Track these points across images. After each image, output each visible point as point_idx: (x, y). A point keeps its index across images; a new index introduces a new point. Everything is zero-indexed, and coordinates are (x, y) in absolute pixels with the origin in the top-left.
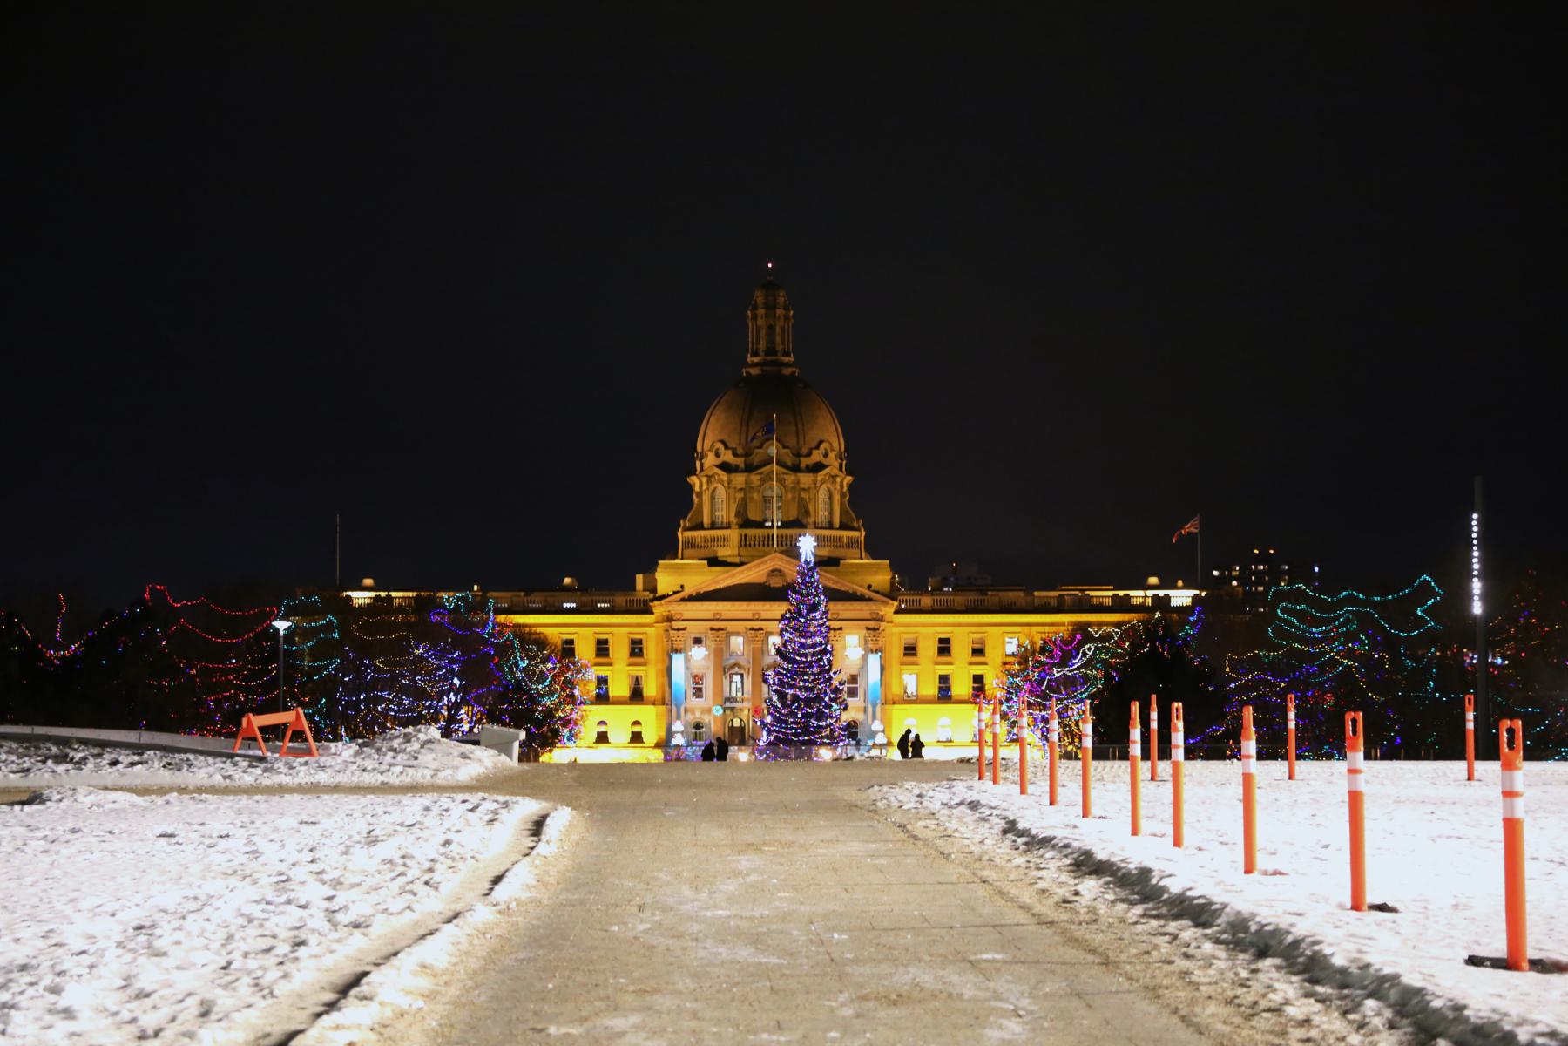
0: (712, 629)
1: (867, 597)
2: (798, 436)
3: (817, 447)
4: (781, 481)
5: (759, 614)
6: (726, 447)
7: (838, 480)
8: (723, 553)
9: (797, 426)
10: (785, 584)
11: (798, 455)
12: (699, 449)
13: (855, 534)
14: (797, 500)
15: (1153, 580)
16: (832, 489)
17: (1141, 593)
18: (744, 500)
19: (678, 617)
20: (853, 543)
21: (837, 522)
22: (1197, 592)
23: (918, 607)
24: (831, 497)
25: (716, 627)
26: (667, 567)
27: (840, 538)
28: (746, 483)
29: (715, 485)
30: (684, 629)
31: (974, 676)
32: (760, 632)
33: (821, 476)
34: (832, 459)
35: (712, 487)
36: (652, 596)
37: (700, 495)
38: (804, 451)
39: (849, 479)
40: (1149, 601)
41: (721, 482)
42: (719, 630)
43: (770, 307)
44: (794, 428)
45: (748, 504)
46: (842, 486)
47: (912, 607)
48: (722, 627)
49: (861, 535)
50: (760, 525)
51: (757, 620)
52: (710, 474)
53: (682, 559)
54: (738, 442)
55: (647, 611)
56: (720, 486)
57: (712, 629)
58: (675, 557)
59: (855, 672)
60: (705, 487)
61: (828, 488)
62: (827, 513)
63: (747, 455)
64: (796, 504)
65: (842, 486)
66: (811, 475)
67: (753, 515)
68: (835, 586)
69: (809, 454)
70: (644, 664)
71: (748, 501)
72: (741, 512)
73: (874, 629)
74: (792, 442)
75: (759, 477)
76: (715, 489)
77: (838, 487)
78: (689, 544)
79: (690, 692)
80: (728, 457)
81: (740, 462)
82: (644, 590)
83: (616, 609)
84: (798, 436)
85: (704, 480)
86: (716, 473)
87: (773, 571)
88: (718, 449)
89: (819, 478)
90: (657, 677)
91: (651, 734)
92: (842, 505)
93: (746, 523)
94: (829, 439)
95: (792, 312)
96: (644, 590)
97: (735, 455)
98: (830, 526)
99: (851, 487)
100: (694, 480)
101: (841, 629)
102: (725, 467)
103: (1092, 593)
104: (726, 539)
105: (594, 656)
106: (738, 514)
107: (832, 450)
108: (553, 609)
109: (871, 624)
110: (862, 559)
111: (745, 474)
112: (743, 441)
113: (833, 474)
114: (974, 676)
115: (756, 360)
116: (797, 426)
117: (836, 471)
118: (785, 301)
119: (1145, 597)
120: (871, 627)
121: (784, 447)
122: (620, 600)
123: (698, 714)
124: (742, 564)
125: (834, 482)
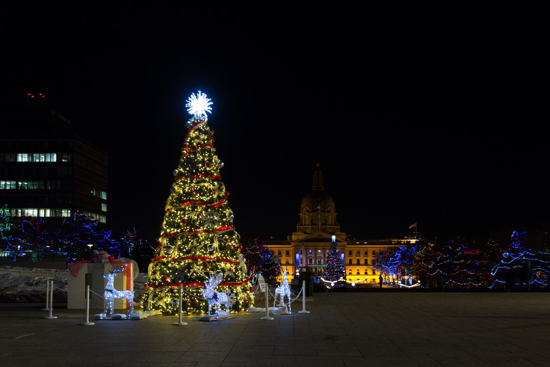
3: (329, 207)
6: (308, 207)
7: (334, 214)
8: (308, 231)
12: (302, 207)
13: (338, 227)
15: (406, 237)
17: (403, 240)
20: (337, 229)
21: (333, 224)
22: (416, 240)
24: (332, 218)
26: (294, 234)
27: (334, 227)
30: (299, 248)
33: (330, 213)
34: (332, 209)
36: (291, 241)
37: (302, 218)
38: (326, 208)
39: (336, 214)
40: (405, 242)
41: (307, 215)
46: (334, 216)
49: (339, 227)
50: (316, 225)
51: (316, 246)
53: (298, 232)
55: (290, 244)
58: (296, 232)
60: (303, 216)
61: (332, 216)
62: (331, 222)
65: (334, 216)
67: (314, 222)
69: (327, 208)
70: (290, 256)
72: (311, 222)
73: (343, 249)
76: (305, 216)
77: (334, 216)
78: (299, 229)
81: (311, 210)
82: (289, 239)
85: (303, 214)
90: (292, 259)
91: (291, 273)
92: (334, 220)
93: (313, 224)
94: (332, 206)
96: (289, 239)
97: (310, 208)
98: (332, 225)
99: (337, 216)
100: (301, 214)
102: (308, 211)
103: (393, 240)
104: (308, 228)
106: (311, 222)
109: (342, 247)
110: (339, 232)
115: (315, 187)
117: (333, 212)
119: (404, 241)
121: (322, 207)
122: (284, 242)
124: (312, 234)
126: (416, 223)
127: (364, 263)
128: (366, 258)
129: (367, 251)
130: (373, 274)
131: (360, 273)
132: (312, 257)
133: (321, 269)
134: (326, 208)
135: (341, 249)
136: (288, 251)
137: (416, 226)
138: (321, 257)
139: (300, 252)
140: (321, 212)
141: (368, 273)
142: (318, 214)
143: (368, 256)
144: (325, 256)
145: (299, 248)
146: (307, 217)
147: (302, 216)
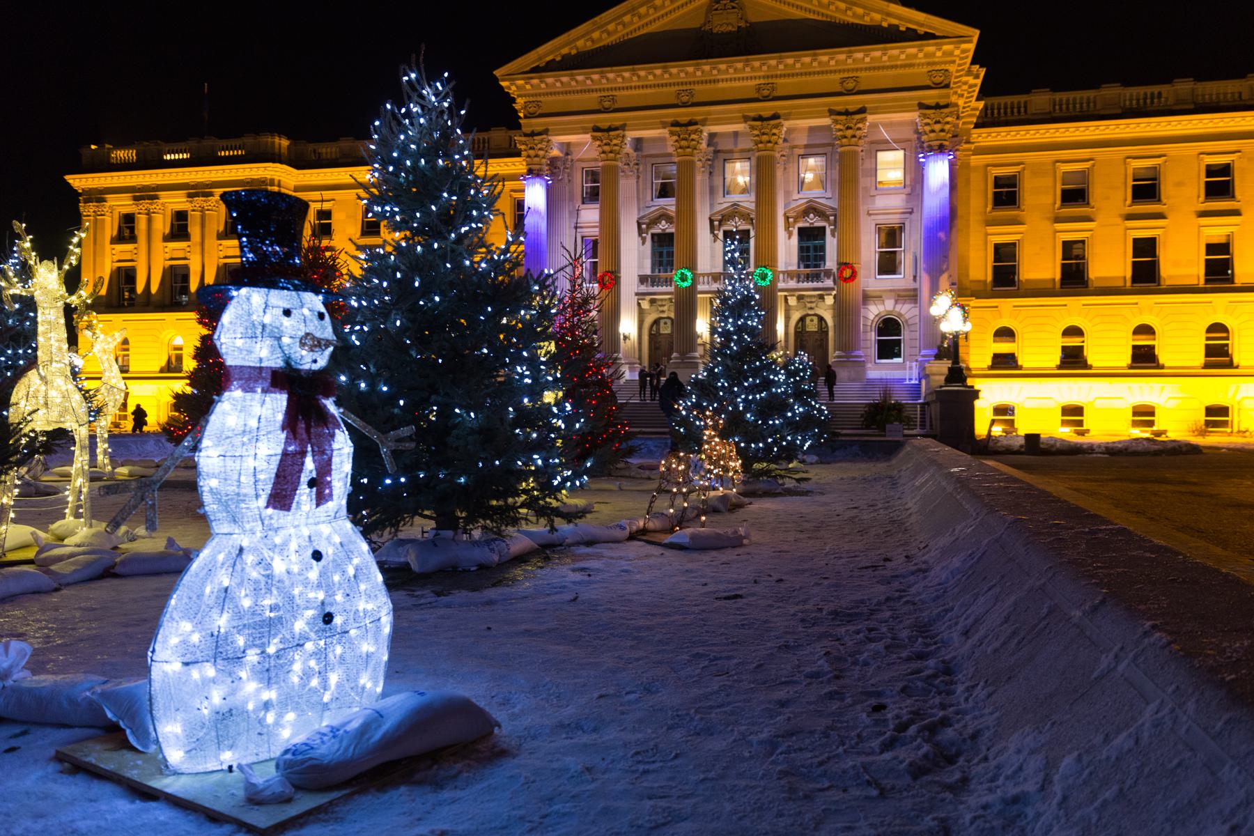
0: (596, 129)
1: (921, 30)
10: (742, 24)
19: (532, 110)
23: (1023, 116)
25: (605, 125)
31: (1136, 241)
32: (691, 128)
42: (610, 129)
48: (617, 124)
51: (685, 105)
57: (596, 129)
59: (894, 220)
73: (938, 107)
114: (1136, 241)
120: (932, 102)
127: (1129, 274)
128: (1144, 230)
129: (1154, 168)
130: (1207, 366)
131: (1093, 357)
141: (1162, 359)
143: (1160, 216)
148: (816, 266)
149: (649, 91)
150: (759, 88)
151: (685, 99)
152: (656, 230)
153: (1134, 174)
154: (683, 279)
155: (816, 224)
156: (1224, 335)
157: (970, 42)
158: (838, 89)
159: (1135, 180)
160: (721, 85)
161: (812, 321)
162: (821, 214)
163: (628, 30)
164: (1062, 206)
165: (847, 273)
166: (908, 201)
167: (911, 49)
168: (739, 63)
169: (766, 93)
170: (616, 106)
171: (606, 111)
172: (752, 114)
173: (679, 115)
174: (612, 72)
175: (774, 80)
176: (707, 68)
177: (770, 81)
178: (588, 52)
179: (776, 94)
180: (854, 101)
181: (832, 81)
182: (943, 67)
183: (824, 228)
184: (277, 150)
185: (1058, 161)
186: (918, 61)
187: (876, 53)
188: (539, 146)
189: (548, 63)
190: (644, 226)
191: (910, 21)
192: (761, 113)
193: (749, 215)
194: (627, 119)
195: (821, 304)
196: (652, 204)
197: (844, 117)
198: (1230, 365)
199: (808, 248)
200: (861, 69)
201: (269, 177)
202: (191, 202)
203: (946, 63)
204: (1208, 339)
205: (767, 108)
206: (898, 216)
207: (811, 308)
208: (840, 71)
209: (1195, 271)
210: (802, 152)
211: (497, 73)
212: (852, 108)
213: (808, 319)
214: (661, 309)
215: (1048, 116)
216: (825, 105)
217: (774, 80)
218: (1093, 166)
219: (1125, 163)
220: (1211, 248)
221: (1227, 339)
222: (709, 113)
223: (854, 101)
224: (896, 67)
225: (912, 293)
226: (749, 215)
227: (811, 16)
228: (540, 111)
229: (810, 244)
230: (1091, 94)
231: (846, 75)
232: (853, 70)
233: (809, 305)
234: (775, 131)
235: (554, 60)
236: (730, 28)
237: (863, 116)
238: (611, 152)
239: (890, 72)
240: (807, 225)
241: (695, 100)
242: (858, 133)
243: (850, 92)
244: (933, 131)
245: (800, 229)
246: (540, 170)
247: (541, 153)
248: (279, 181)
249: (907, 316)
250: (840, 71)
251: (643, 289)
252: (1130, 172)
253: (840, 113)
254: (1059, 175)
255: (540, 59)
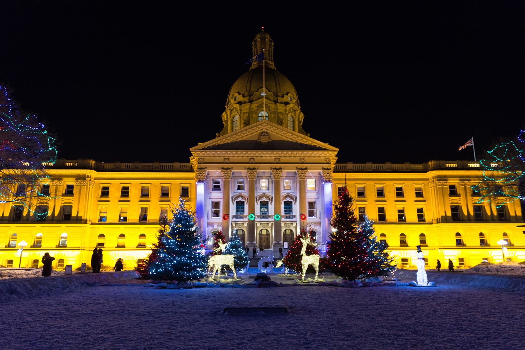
0: (223, 168)
1: (323, 148)
2: (276, 87)
3: (287, 94)
4: (268, 108)
5: (254, 160)
6: (239, 94)
7: (297, 113)
9: (276, 82)
10: (270, 141)
11: (277, 96)
12: (227, 101)
14: (276, 118)
16: (294, 117)
18: (248, 118)
19: (201, 161)
23: (345, 170)
25: (226, 167)
28: (249, 109)
29: (234, 114)
31: (379, 208)
32: (254, 170)
35: (232, 115)
37: (226, 122)
39: (302, 114)
41: (237, 111)
42: (227, 169)
43: (263, 40)
44: (274, 83)
45: (250, 120)
46: (299, 118)
47: (340, 170)
48: (230, 167)
51: (252, 163)
52: (231, 109)
54: (246, 90)
56: (236, 113)
57: (223, 168)
60: (229, 116)
61: (292, 117)
63: (250, 96)
64: (276, 120)
66: (284, 105)
68: (302, 142)
69: (283, 97)
71: (250, 118)
73: (328, 169)
74: (274, 89)
75: (256, 105)
76: (234, 116)
77: (297, 117)
79: (211, 213)
80: (240, 98)
81: (246, 99)
83: (173, 170)
84: (276, 87)
85: (229, 112)
86: (234, 107)
87: (262, 133)
88: (236, 97)
89: (288, 109)
95: (273, 44)
97: (244, 96)
101: (306, 169)
102: (240, 103)
105: (160, 196)
107: (294, 98)
108: (138, 169)
111: (249, 104)
112: (248, 90)
113: (295, 109)
114: (379, 208)
116: (276, 82)
117: (296, 107)
118: (270, 39)
121: (269, 91)
122: (176, 165)
123: (215, 227)
125: (296, 114)
126: (472, 139)
128: (381, 205)
130: (401, 246)
132: (242, 197)
133: (269, 230)
134: (280, 94)
135: (321, 171)
136: (187, 189)
137: (473, 145)
138: (268, 197)
139: (212, 184)
140: (268, 101)
142: (260, 107)
143: (385, 201)
144: (279, 194)
145: (205, 168)
146: (237, 117)
147: (227, 118)
148: (289, 214)
149: (241, 158)
150: (275, 160)
151: (252, 161)
152: (238, 200)
153: (377, 189)
154: (252, 217)
155: (289, 201)
156: (405, 237)
157: (336, 152)
158: (299, 162)
159: (377, 190)
160: (263, 158)
161: (288, 231)
162: (291, 197)
163: (234, 139)
164: (358, 197)
165: (303, 217)
166: (317, 195)
167: (320, 152)
168: (270, 152)
169: (277, 161)
170: (229, 162)
171: (226, 163)
172: (273, 167)
173: (250, 166)
174: (229, 152)
175: (280, 158)
176: (260, 153)
177: (279, 158)
178: (221, 145)
179: (281, 162)
180: (304, 166)
181: (297, 160)
182: (329, 158)
183: (292, 202)
184: (91, 165)
185: (356, 184)
186: (322, 156)
187: (310, 153)
188: (203, 173)
189: (208, 147)
190: (234, 199)
191: (320, 145)
192: (276, 167)
193: (268, 197)
194: (233, 166)
195: (291, 226)
196: (236, 192)
197: (301, 170)
198: (407, 246)
199: (287, 208)
200: (306, 157)
201: (87, 174)
202: (53, 182)
203: (330, 157)
204: (400, 238)
205: (278, 166)
206: (314, 199)
207: (289, 227)
208: (299, 157)
209: (395, 218)
210: (285, 178)
211: (191, 149)
212: (303, 168)
213: (287, 230)
214: (239, 226)
215: (353, 170)
216: (295, 166)
217: (280, 158)
218: (366, 186)
219: (374, 185)
220: (399, 211)
221: (405, 238)
222: (260, 166)
223: (304, 166)
224: (316, 157)
225: (319, 223)
226: (268, 197)
227: (291, 140)
228: (204, 162)
229: (288, 206)
230: (364, 165)
231: (301, 158)
232: (303, 157)
233: (288, 226)
234: (280, 173)
235: (210, 146)
236: (266, 141)
237: (306, 170)
238: (227, 176)
239: (314, 158)
240: (287, 201)
241: (255, 162)
242: (305, 175)
243: (302, 163)
244: (327, 176)
245: (284, 202)
246: (203, 180)
247: (204, 175)
248: (90, 176)
249: (318, 230)
250: (299, 157)
251: (234, 219)
252: (376, 188)
253: (300, 169)
254: (357, 188)
255: (206, 146)
